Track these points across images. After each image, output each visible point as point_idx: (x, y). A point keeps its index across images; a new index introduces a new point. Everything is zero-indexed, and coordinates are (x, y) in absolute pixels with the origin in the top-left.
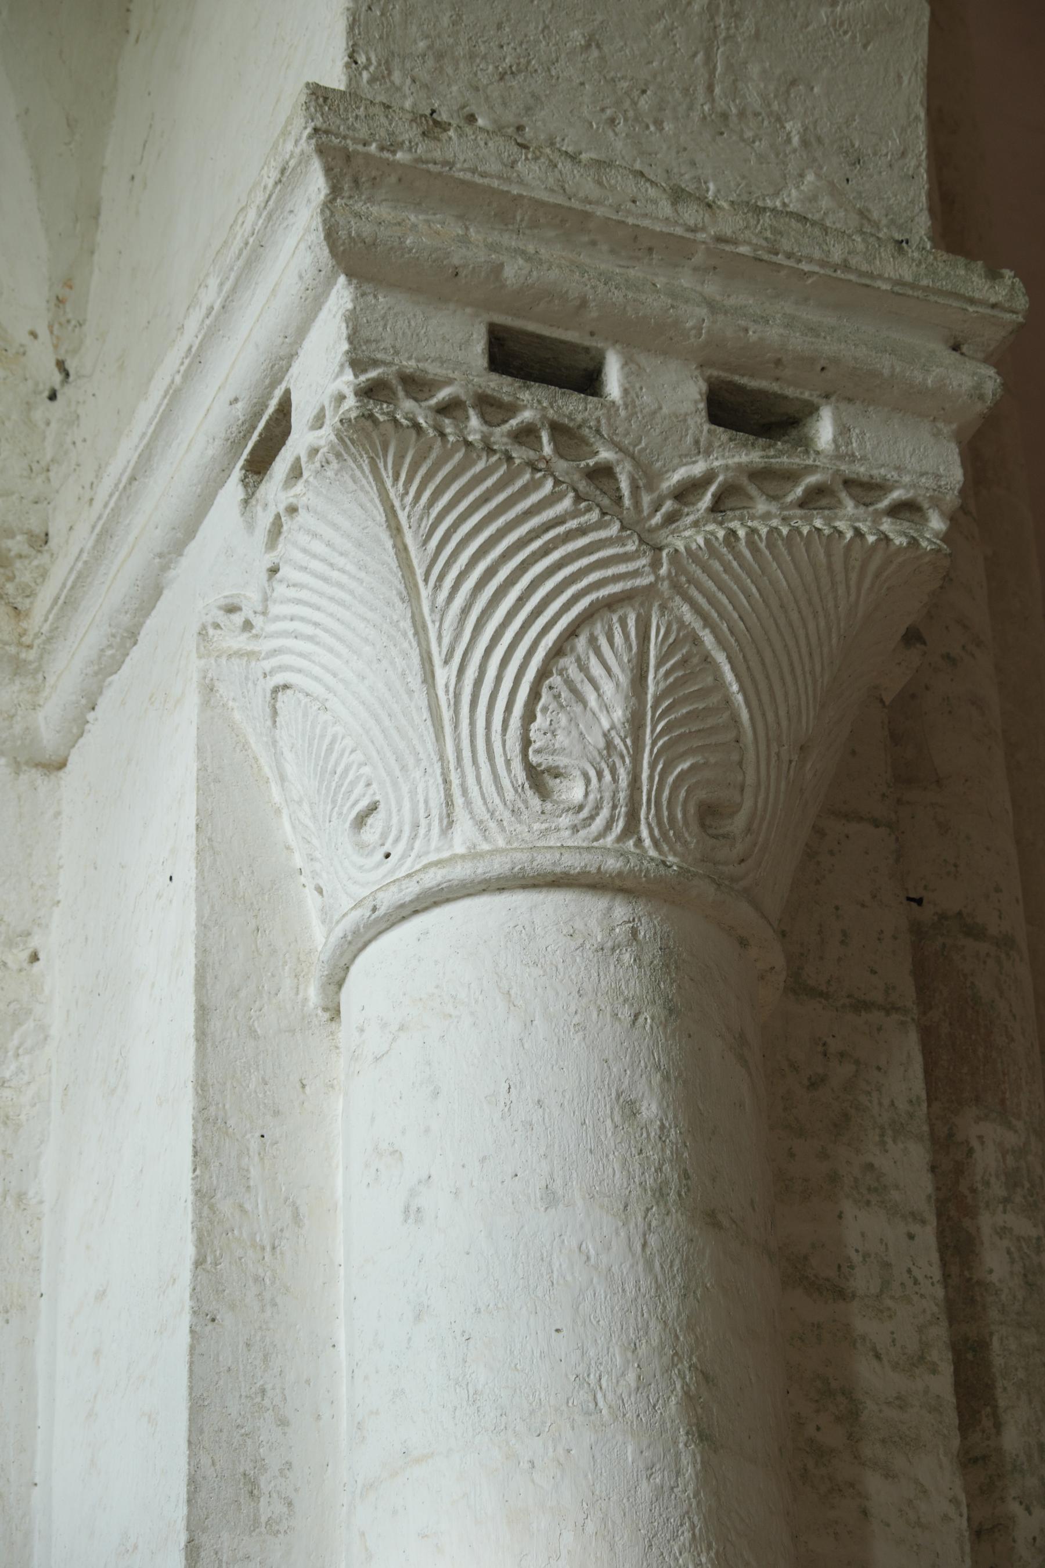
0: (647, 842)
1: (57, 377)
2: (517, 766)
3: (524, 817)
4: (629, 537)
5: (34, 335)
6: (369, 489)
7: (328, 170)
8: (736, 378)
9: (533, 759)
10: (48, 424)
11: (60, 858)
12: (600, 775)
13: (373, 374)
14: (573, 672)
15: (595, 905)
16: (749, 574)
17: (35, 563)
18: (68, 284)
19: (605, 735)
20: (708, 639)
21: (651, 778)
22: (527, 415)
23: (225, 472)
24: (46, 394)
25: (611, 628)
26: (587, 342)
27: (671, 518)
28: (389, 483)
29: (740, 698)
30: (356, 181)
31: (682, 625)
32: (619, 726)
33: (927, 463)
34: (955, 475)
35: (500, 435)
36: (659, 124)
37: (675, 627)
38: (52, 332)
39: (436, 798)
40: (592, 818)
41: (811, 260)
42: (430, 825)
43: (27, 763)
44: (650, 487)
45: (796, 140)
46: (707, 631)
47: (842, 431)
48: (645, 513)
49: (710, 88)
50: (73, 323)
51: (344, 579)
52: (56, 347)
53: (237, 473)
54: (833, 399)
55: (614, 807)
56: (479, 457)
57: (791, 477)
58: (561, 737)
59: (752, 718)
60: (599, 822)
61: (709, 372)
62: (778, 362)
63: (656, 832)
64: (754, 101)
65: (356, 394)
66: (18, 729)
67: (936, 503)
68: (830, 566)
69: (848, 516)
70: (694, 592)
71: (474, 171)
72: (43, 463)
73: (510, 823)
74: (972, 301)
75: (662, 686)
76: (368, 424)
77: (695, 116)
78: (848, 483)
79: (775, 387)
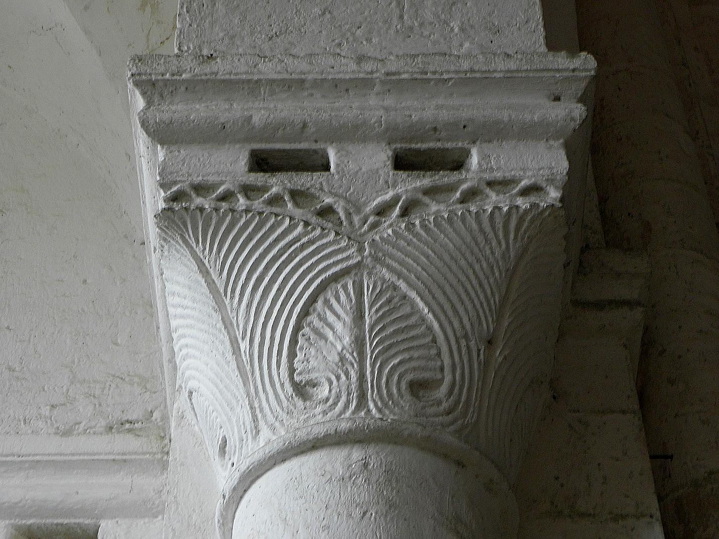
0: (374, 411)
2: (288, 385)
3: (295, 414)
4: (341, 239)
6: (185, 254)
7: (143, 94)
8: (413, 146)
9: (297, 378)
12: (338, 378)
13: (175, 189)
14: (317, 323)
16: (426, 243)
19: (339, 354)
20: (402, 285)
21: (372, 372)
22: (274, 190)
25: (337, 292)
26: (314, 146)
27: (374, 226)
28: (194, 245)
29: (430, 316)
30: (161, 96)
31: (384, 281)
32: (347, 347)
36: (369, 40)
37: (379, 283)
39: (248, 419)
40: (335, 404)
41: (448, 72)
42: (247, 437)
44: (358, 210)
45: (456, 30)
46: (401, 281)
47: (484, 157)
48: (357, 227)
49: (401, 17)
51: (187, 311)
54: (478, 143)
55: (349, 394)
56: (241, 217)
57: (451, 188)
59: (441, 326)
60: (340, 405)
61: (394, 146)
62: (435, 129)
63: (379, 403)
64: (429, 16)
65: (165, 201)
67: (551, 181)
68: (482, 230)
70: (389, 261)
71: (230, 73)
73: (287, 420)
74: (558, 70)
75: (374, 318)
76: (169, 213)
77: (392, 32)
78: (490, 184)
79: (439, 145)
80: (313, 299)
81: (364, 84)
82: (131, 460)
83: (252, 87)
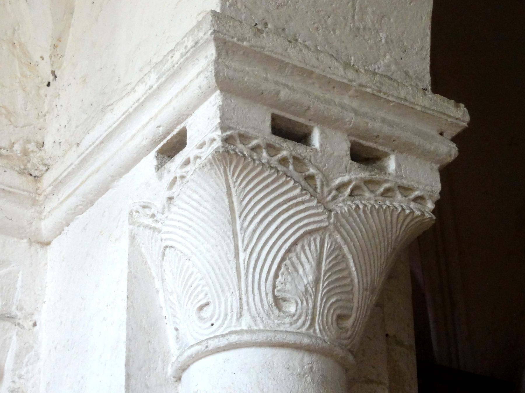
0: (318, 331)
1: (51, 78)
2: (270, 296)
3: (271, 317)
4: (321, 206)
5: (42, 58)
6: (221, 178)
7: (217, 47)
9: (277, 293)
10: (46, 96)
11: (46, 283)
12: (302, 303)
13: (229, 133)
14: (294, 259)
15: (297, 356)
16: (363, 223)
17: (38, 155)
18: (59, 40)
19: (305, 286)
20: (346, 249)
21: (321, 305)
22: (284, 153)
23: (149, 151)
24: (46, 83)
25: (310, 242)
26: (307, 123)
27: (334, 198)
28: (230, 177)
29: (355, 273)
30: (227, 52)
31: (337, 243)
32: (310, 283)
33: (428, 183)
34: (438, 187)
35: (274, 162)
36: (334, 30)
37: (334, 243)
38: (51, 59)
39: (236, 305)
40: (298, 320)
41: (392, 96)
42: (232, 315)
43: (34, 242)
44: (328, 185)
45: (383, 41)
46: (346, 246)
47: (399, 165)
48: (325, 195)
49: (353, 17)
50: (59, 56)
51: (206, 211)
52: (52, 65)
53: (154, 153)
54: (396, 152)
55: (306, 316)
56: (267, 170)
57: (378, 183)
58: (287, 286)
59: (359, 282)
60: (300, 322)
62: (378, 136)
63: (321, 327)
64: (369, 24)
65: (222, 141)
66: (33, 228)
67: (430, 197)
68: (391, 222)
69: (399, 201)
70: (342, 230)
71: (272, 51)
72: (43, 113)
73: (266, 319)
74: (449, 116)
75: (328, 267)
76: (226, 154)
77: (348, 28)
78: (400, 187)
79: (374, 146)
80: (295, 243)
81: (344, 87)
82: (14, 193)
83: (280, 65)
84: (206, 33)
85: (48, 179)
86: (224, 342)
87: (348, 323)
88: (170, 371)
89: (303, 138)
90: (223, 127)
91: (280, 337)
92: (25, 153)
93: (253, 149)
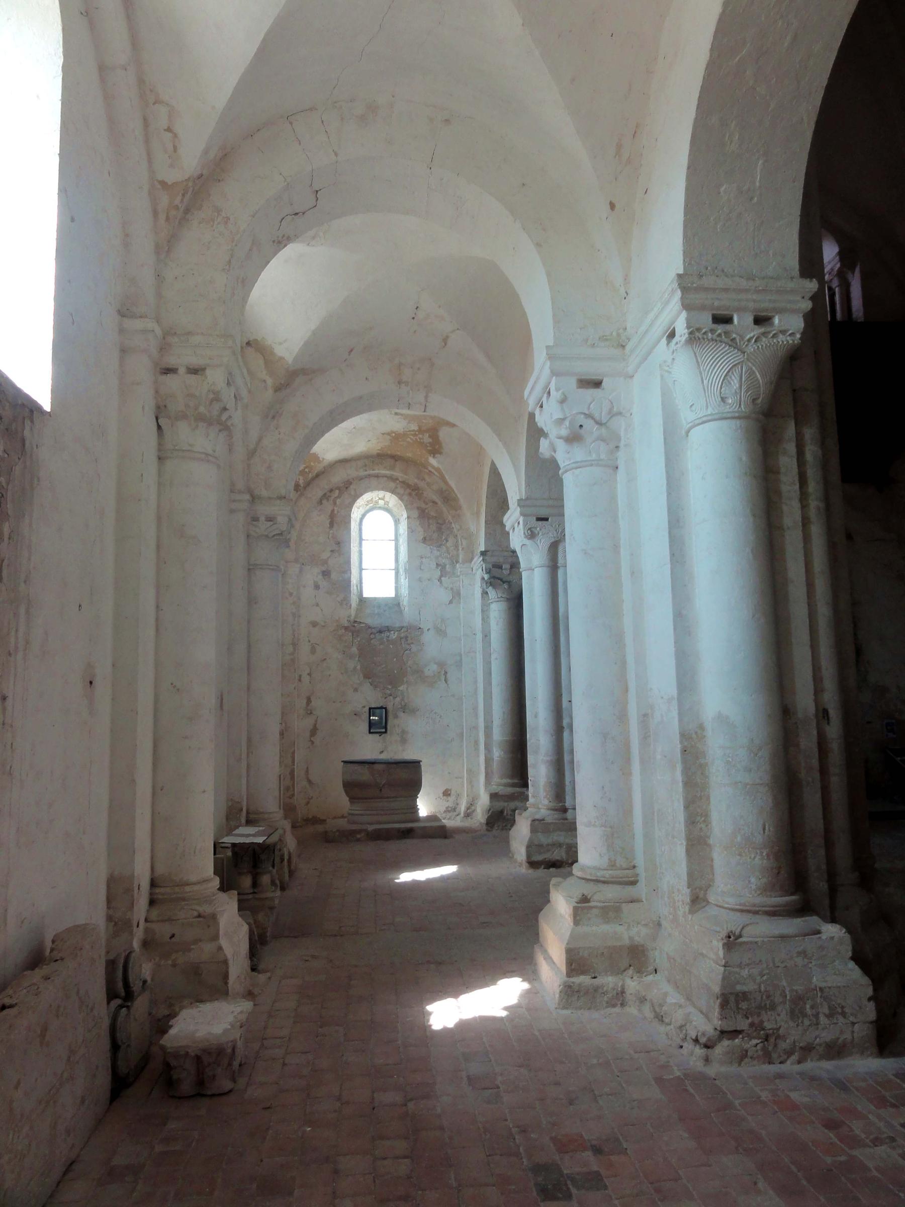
15: (734, 421)
22: (719, 331)
33: (796, 324)
34: (802, 325)
35: (715, 337)
47: (780, 320)
57: (769, 332)
58: (726, 391)
80: (728, 372)
84: (675, 285)
85: (628, 348)
86: (700, 421)
87: (759, 401)
88: (683, 432)
89: (728, 320)
90: (688, 327)
91: (725, 415)
92: (619, 335)
93: (705, 333)
